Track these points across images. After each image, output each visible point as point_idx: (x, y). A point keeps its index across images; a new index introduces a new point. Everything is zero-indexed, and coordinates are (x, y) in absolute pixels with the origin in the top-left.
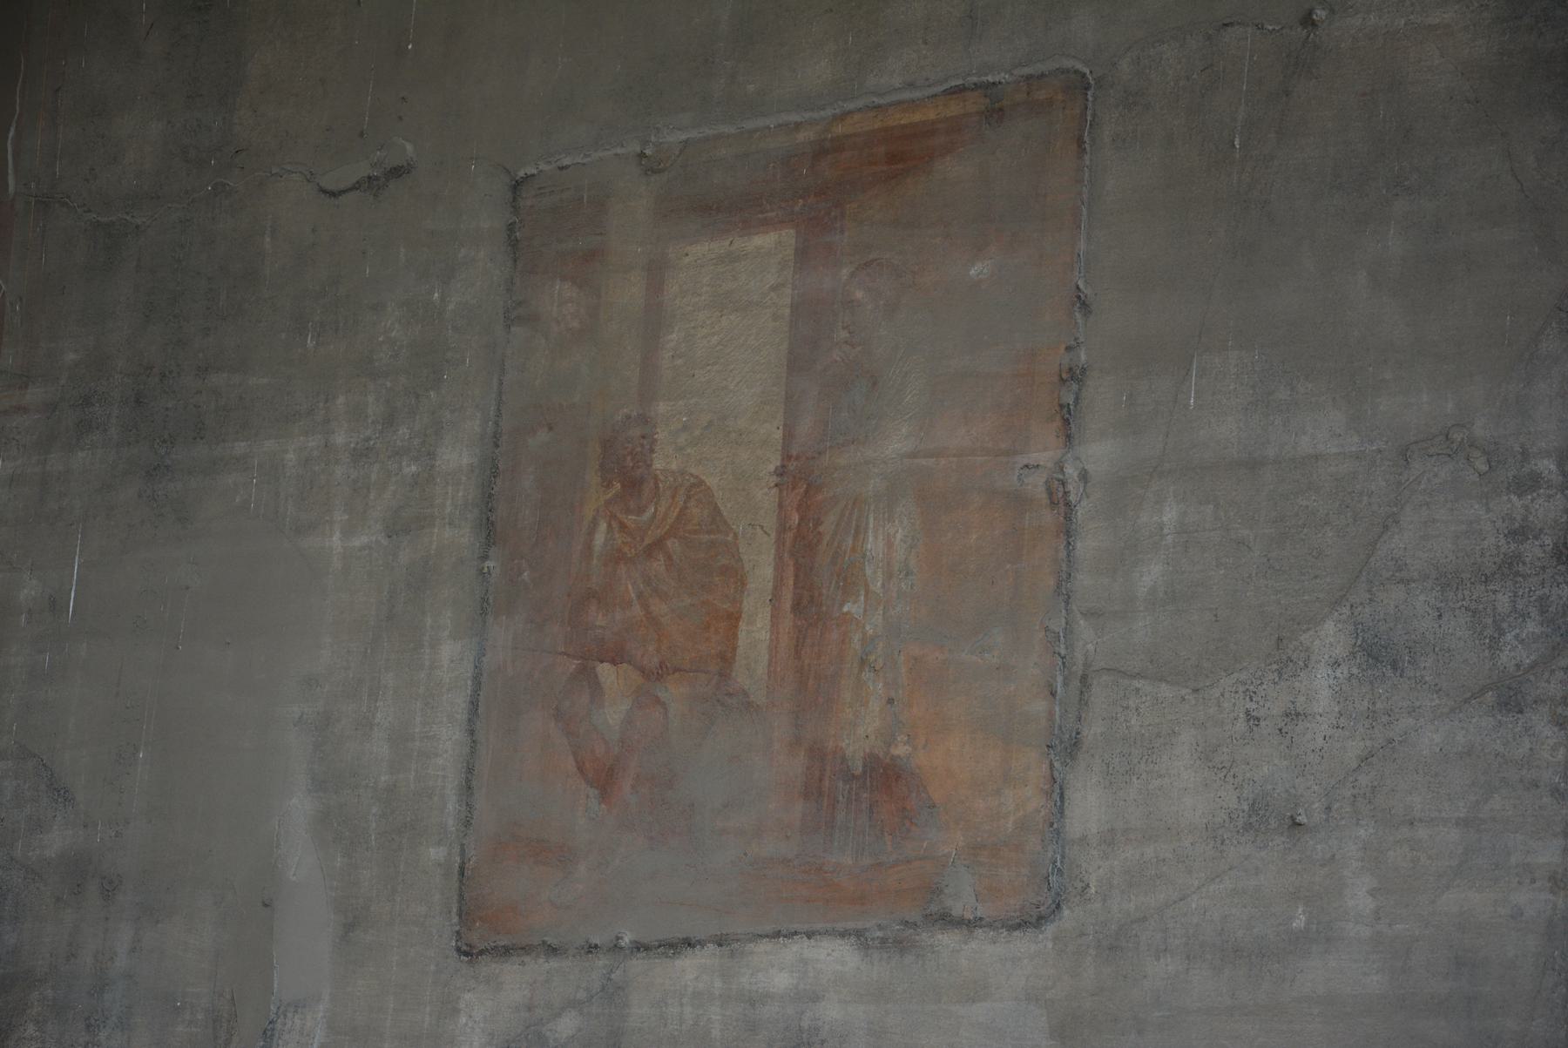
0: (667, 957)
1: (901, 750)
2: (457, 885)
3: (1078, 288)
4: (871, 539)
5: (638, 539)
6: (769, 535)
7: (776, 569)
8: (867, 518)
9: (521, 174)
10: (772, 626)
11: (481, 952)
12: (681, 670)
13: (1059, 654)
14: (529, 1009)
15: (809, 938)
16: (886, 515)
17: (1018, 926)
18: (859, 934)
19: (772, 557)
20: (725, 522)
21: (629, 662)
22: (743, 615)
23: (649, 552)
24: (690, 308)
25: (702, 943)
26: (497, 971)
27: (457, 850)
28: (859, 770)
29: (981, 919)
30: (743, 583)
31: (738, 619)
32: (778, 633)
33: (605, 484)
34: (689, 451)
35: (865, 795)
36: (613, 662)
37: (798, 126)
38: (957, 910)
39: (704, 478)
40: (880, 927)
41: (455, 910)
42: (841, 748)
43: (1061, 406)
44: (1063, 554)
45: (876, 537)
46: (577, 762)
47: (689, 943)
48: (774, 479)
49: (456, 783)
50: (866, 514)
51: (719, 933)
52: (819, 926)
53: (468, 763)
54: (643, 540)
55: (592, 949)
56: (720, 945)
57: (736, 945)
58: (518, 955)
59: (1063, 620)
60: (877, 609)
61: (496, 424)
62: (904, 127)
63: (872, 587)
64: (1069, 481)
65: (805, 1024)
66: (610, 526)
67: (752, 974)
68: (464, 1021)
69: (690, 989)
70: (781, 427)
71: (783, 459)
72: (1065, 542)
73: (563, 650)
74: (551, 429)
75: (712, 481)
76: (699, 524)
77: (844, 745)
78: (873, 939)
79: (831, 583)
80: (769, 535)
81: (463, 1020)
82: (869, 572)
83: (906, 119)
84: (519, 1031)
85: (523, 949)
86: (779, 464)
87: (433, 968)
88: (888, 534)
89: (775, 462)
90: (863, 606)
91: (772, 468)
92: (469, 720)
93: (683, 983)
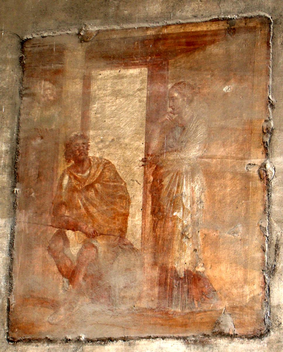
1: (200, 269)
2: (7, 314)
3: (269, 98)
8: (183, 180)
11: (18, 341)
16: (191, 180)
19: (142, 193)
20: (121, 179)
21: (80, 230)
22: (130, 214)
23: (88, 188)
27: (6, 300)
30: (129, 202)
35: (185, 286)
42: (175, 267)
43: (264, 143)
49: (5, 274)
53: (10, 267)
54: (84, 183)
58: (35, 343)
63: (185, 206)
66: (70, 177)
71: (145, 156)
75: (114, 162)
77: (176, 266)
79: (168, 204)
82: (184, 200)
86: (143, 157)
89: (142, 156)
91: (141, 159)
92: (10, 250)
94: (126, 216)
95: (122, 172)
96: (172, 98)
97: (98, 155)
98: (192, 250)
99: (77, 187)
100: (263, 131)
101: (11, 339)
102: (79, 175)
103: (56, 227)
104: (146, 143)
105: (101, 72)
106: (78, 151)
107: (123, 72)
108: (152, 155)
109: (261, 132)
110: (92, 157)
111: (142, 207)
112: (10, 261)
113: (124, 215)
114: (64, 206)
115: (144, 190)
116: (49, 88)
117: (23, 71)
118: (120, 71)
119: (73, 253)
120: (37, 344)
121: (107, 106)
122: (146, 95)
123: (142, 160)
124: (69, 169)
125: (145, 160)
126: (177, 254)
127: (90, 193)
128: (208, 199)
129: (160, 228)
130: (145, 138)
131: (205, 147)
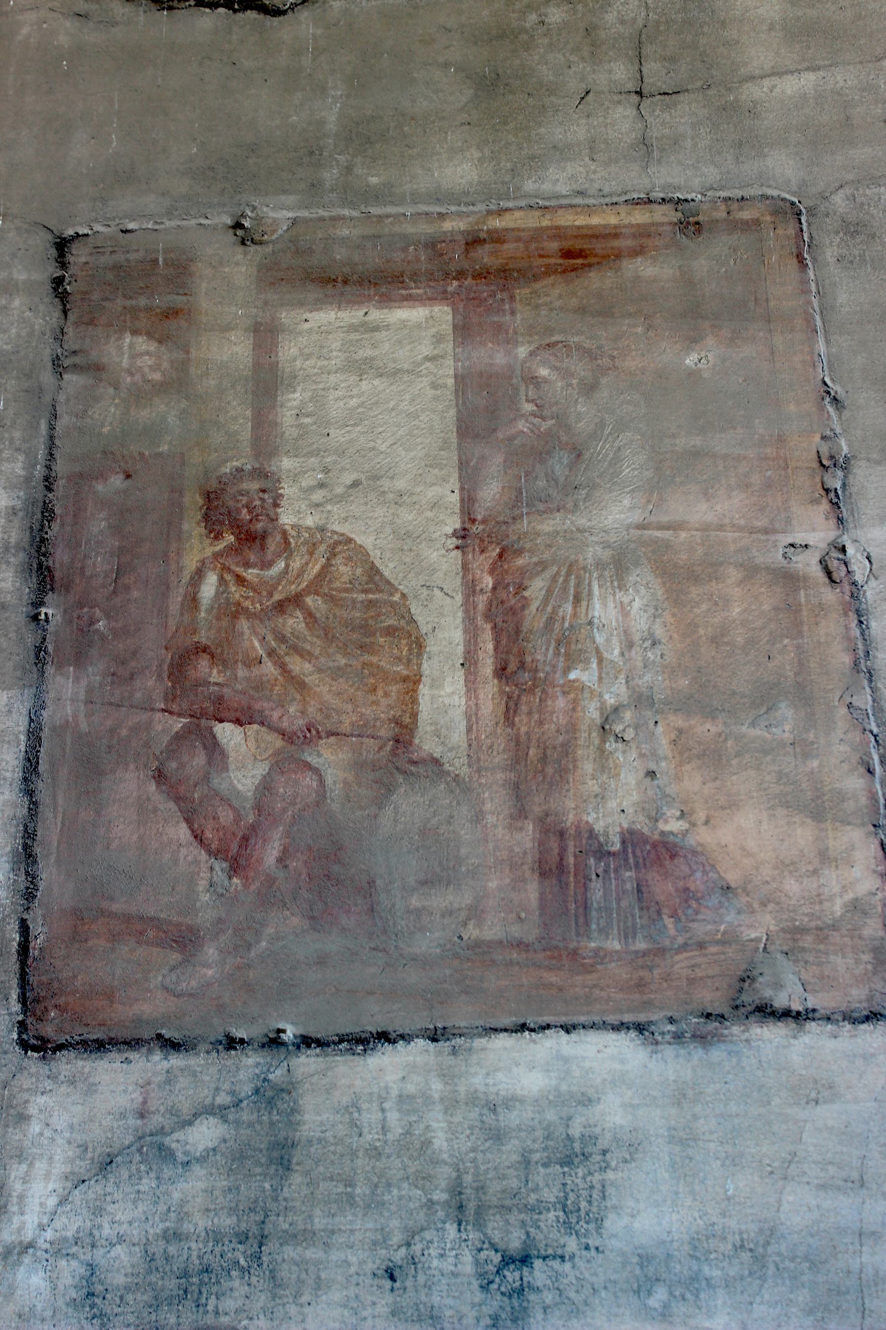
1: (673, 826)
2: (17, 966)
3: (825, 384)
4: (597, 606)
5: (265, 593)
6: (453, 597)
7: (466, 631)
8: (590, 584)
9: (71, 232)
10: (468, 690)
11: (61, 1047)
12: (338, 734)
13: (871, 732)
14: (142, 1116)
15: (568, 1032)
16: (616, 584)
17: (867, 1019)
18: (640, 1028)
19: (459, 620)
20: (388, 582)
21: (262, 724)
22: (423, 679)
23: (281, 607)
24: (316, 370)
26: (87, 1070)
28: (617, 847)
29: (814, 1010)
30: (418, 645)
31: (417, 682)
32: (477, 698)
33: (212, 535)
34: (329, 508)
35: (628, 874)
36: (238, 722)
37: (442, 216)
38: (780, 1001)
39: (352, 536)
40: (671, 1020)
41: (14, 995)
42: (587, 822)
43: (827, 491)
46: (193, 831)
47: (384, 1037)
48: (453, 542)
49: (8, 849)
51: (432, 1027)
52: (582, 1019)
53: (26, 827)
54: (271, 594)
55: (232, 1043)
56: (434, 1040)
57: (459, 1041)
59: (869, 698)
60: (617, 678)
61: (49, 468)
62: (579, 228)
63: (605, 655)
64: (853, 561)
65: (576, 1131)
66: (222, 580)
67: (488, 1074)
68: (37, 1129)
69: (394, 1093)
71: (463, 522)
72: (856, 622)
73: (163, 706)
74: (128, 476)
75: (365, 540)
76: (351, 583)
77: (590, 819)
78: (663, 1034)
79: (547, 649)
80: (453, 597)
81: (35, 1127)
82: (600, 639)
83: (581, 221)
84: (127, 1143)
85: (125, 1043)
86: (458, 526)
89: (454, 523)
90: (596, 674)
91: (449, 530)
92: (25, 779)
93: (382, 1084)
94: (412, 682)
95: (391, 565)
96: (533, 380)
97: (310, 522)
98: (641, 774)
99: (247, 604)
100: (821, 462)
101: (33, 1041)
102: (251, 574)
103: (180, 715)
104: (462, 489)
105: (307, 315)
106: (245, 511)
107: (376, 315)
108: (484, 521)
109: (816, 465)
110: (293, 526)
111: (465, 658)
112: (25, 811)
113: (405, 679)
114: (205, 655)
115: (466, 611)
116: (148, 353)
117: (65, 312)
120: (126, 1055)
121: (331, 397)
122: (452, 372)
123: (455, 534)
124: (216, 556)
125: (462, 533)
126: (592, 786)
127: (290, 621)
128: (675, 636)
129: (530, 713)
130: (460, 477)
131: (649, 502)
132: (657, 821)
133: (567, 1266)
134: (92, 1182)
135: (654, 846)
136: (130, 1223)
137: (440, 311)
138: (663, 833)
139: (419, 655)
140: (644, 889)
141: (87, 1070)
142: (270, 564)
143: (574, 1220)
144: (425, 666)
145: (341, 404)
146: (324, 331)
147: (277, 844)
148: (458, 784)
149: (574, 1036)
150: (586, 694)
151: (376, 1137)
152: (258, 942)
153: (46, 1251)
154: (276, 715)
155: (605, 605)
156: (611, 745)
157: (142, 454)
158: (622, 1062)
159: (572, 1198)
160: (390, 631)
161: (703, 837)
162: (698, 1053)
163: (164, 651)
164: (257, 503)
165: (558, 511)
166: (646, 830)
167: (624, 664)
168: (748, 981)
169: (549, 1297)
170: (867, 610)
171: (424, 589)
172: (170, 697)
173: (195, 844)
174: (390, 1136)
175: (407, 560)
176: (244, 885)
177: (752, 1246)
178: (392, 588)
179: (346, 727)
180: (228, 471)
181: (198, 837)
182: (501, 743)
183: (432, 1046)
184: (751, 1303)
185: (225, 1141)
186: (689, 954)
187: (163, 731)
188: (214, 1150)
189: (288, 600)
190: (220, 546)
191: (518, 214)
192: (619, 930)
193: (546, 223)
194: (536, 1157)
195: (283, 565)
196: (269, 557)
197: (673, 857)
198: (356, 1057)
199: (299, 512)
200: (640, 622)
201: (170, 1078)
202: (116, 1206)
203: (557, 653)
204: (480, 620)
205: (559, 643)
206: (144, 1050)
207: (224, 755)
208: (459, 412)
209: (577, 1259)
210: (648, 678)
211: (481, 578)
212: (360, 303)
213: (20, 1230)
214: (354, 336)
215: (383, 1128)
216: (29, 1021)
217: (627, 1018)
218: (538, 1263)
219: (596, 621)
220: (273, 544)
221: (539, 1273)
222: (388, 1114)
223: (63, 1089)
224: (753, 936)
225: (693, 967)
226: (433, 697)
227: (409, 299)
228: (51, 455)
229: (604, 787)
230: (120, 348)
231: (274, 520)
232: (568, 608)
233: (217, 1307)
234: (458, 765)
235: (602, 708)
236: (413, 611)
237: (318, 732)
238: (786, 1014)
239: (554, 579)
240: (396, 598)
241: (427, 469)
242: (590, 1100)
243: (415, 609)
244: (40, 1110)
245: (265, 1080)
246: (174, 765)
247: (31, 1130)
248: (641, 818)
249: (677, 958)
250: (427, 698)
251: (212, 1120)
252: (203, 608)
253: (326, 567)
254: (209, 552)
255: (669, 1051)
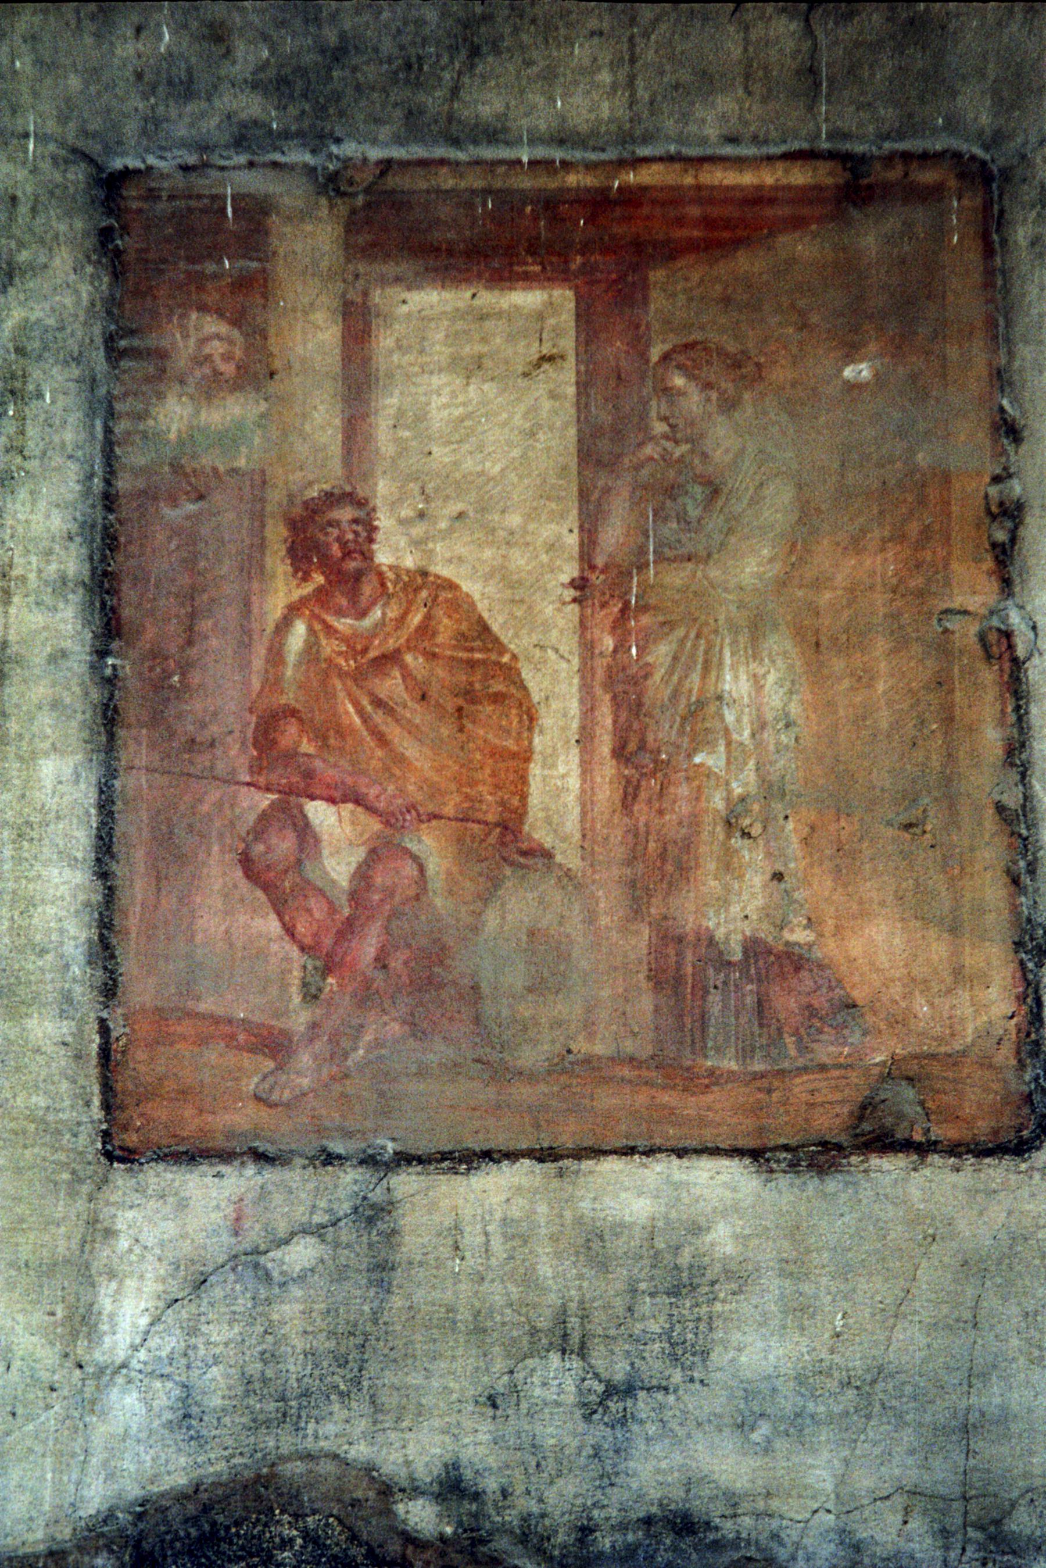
0: (456, 1173)
1: (800, 936)
4: (728, 677)
7: (582, 701)
13: (1020, 835)
15: (680, 1157)
17: (989, 1153)
18: (756, 1154)
19: (575, 689)
21: (357, 802)
25: (512, 1156)
28: (738, 956)
29: (936, 1143)
30: (530, 718)
31: (528, 760)
33: (300, 574)
35: (749, 987)
36: (332, 801)
37: (566, 165)
39: (457, 581)
41: (96, 1102)
42: (707, 928)
44: (1012, 718)
45: (736, 678)
46: (284, 925)
47: (488, 1156)
48: (570, 593)
49: (82, 939)
50: (717, 649)
53: (100, 914)
55: (329, 1159)
56: (541, 1160)
57: (567, 1163)
58: (211, 1165)
61: (108, 482)
62: (728, 188)
63: (735, 737)
65: (685, 1258)
66: (311, 630)
69: (498, 1215)
70: (576, 531)
71: (582, 570)
73: (248, 779)
77: (711, 924)
82: (730, 717)
86: (576, 574)
87: (66, 1176)
88: (755, 676)
89: (570, 571)
90: (724, 756)
91: (565, 578)
92: (98, 860)
93: (487, 1207)
95: (501, 620)
98: (768, 876)
101: (118, 1153)
102: (344, 624)
103: (268, 789)
104: (581, 528)
105: (406, 295)
107: (488, 298)
110: (391, 567)
115: (583, 678)
116: (218, 336)
118: (474, 295)
119: (334, 875)
121: (433, 405)
122: (573, 380)
123: (572, 584)
124: (303, 601)
127: (389, 683)
130: (580, 514)
131: (791, 552)
132: (782, 928)
133: (671, 1398)
134: (185, 1302)
135: (778, 957)
136: (226, 1344)
137: (563, 296)
138: (787, 943)
139: (530, 729)
140: (766, 1005)
141: (177, 1184)
142: (363, 614)
143: (680, 1352)
144: (537, 740)
145: (446, 413)
146: (424, 319)
147: (374, 941)
148: (571, 879)
149: (685, 1162)
150: (713, 782)
151: (480, 1261)
152: (355, 1049)
153: (140, 1371)
154: (373, 792)
155: (736, 678)
156: (737, 842)
157: (215, 470)
158: (735, 1190)
159: (678, 1328)
160: (498, 698)
161: (829, 949)
162: (813, 1184)
163: (248, 715)
164: (350, 536)
165: (689, 560)
166: (770, 939)
167: (756, 748)
168: (870, 1108)
169: (652, 1429)
170: (1028, 692)
171: (537, 651)
172: (256, 768)
173: (287, 938)
174: (493, 1261)
175: (519, 614)
176: (340, 985)
177: (858, 1383)
178: (502, 649)
179: (449, 810)
180: (316, 494)
181: (290, 932)
182: (617, 836)
183: (538, 1167)
184: (855, 1441)
185: (322, 1261)
186: (812, 1077)
187: (250, 808)
188: (312, 1270)
189: (384, 656)
190: (308, 589)
191: (656, 167)
192: (737, 1051)
193: (689, 180)
194: (643, 1286)
195: (379, 613)
196: (364, 600)
197: (798, 969)
198: (459, 1178)
199: (397, 549)
200: (774, 699)
201: (264, 1193)
202: (211, 1327)
203: (681, 732)
204: (599, 691)
205: (684, 719)
206: (237, 1163)
207: (317, 841)
208: (579, 430)
209: (681, 1392)
210: (781, 763)
211: (600, 639)
212: (467, 281)
213: (113, 1349)
214: (460, 325)
215: (487, 1251)
216: (114, 1130)
217: (741, 1143)
218: (642, 1395)
219: (726, 695)
220: (368, 589)
221: (643, 1404)
222: (492, 1238)
223: (152, 1204)
224: (877, 1060)
225: (812, 1092)
226: (544, 778)
227: (528, 280)
228: (110, 465)
229: (728, 889)
230: (183, 327)
231: (367, 556)
232: (695, 677)
233: (316, 1431)
234: (569, 858)
235: (728, 800)
236: (523, 675)
237: (419, 815)
238: (907, 1146)
239: (682, 642)
240: (505, 659)
241: (542, 502)
242: (700, 1228)
243: (526, 674)
244: (130, 1227)
245: (365, 1198)
246: (260, 848)
247: (120, 1246)
248: (765, 926)
249: (798, 1081)
250: (538, 779)
251: (311, 1240)
252: (291, 665)
253: (428, 617)
254: (297, 594)
255: (784, 1181)
